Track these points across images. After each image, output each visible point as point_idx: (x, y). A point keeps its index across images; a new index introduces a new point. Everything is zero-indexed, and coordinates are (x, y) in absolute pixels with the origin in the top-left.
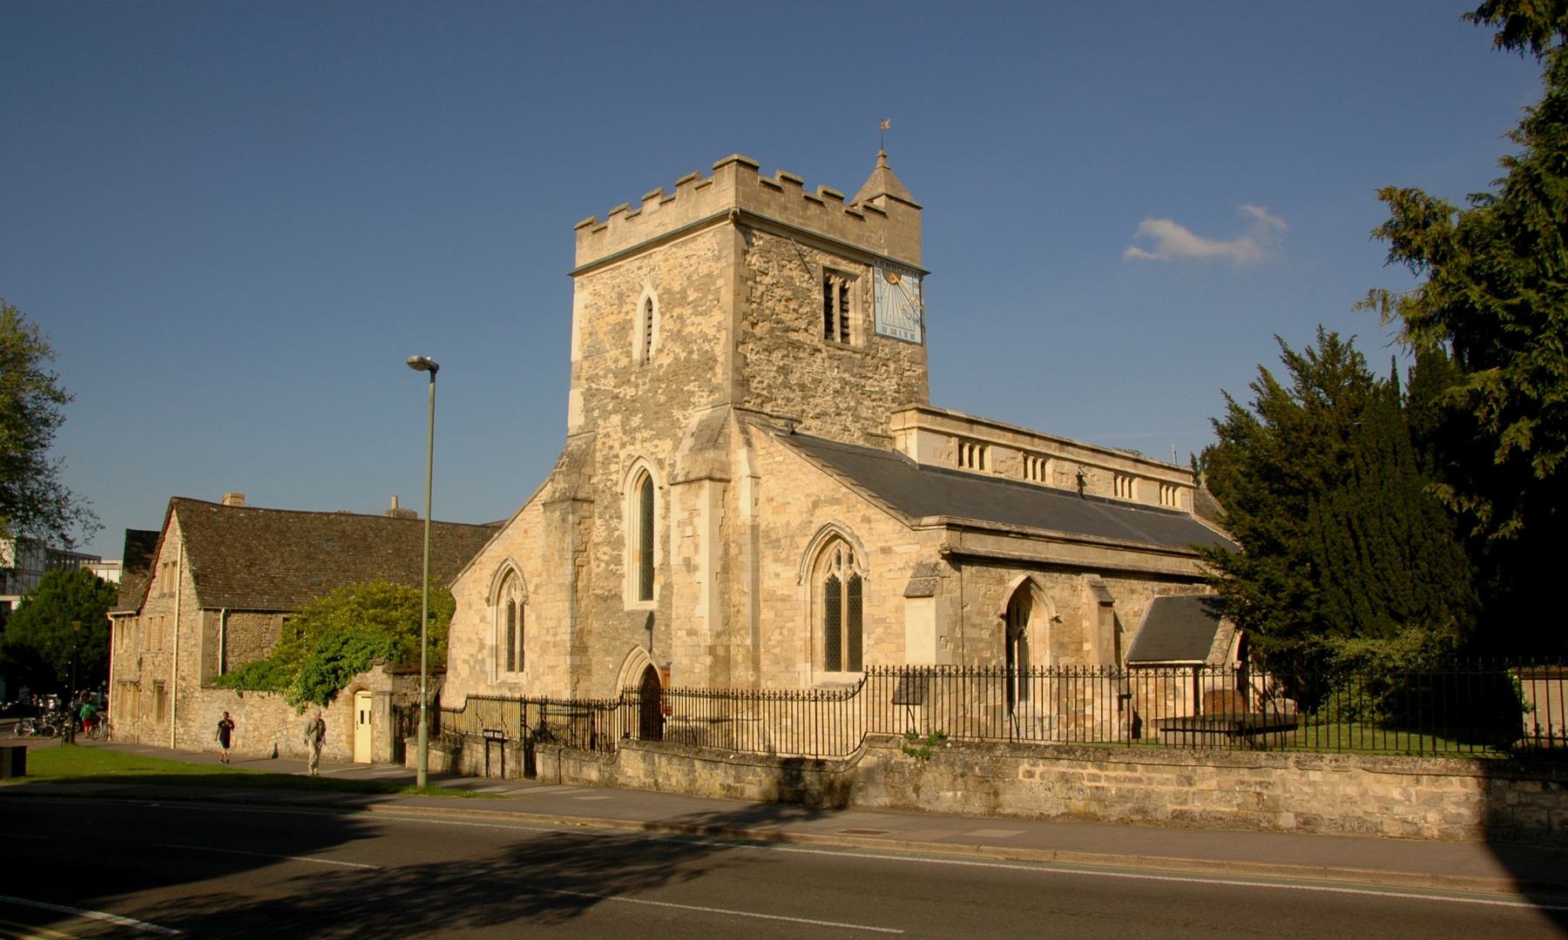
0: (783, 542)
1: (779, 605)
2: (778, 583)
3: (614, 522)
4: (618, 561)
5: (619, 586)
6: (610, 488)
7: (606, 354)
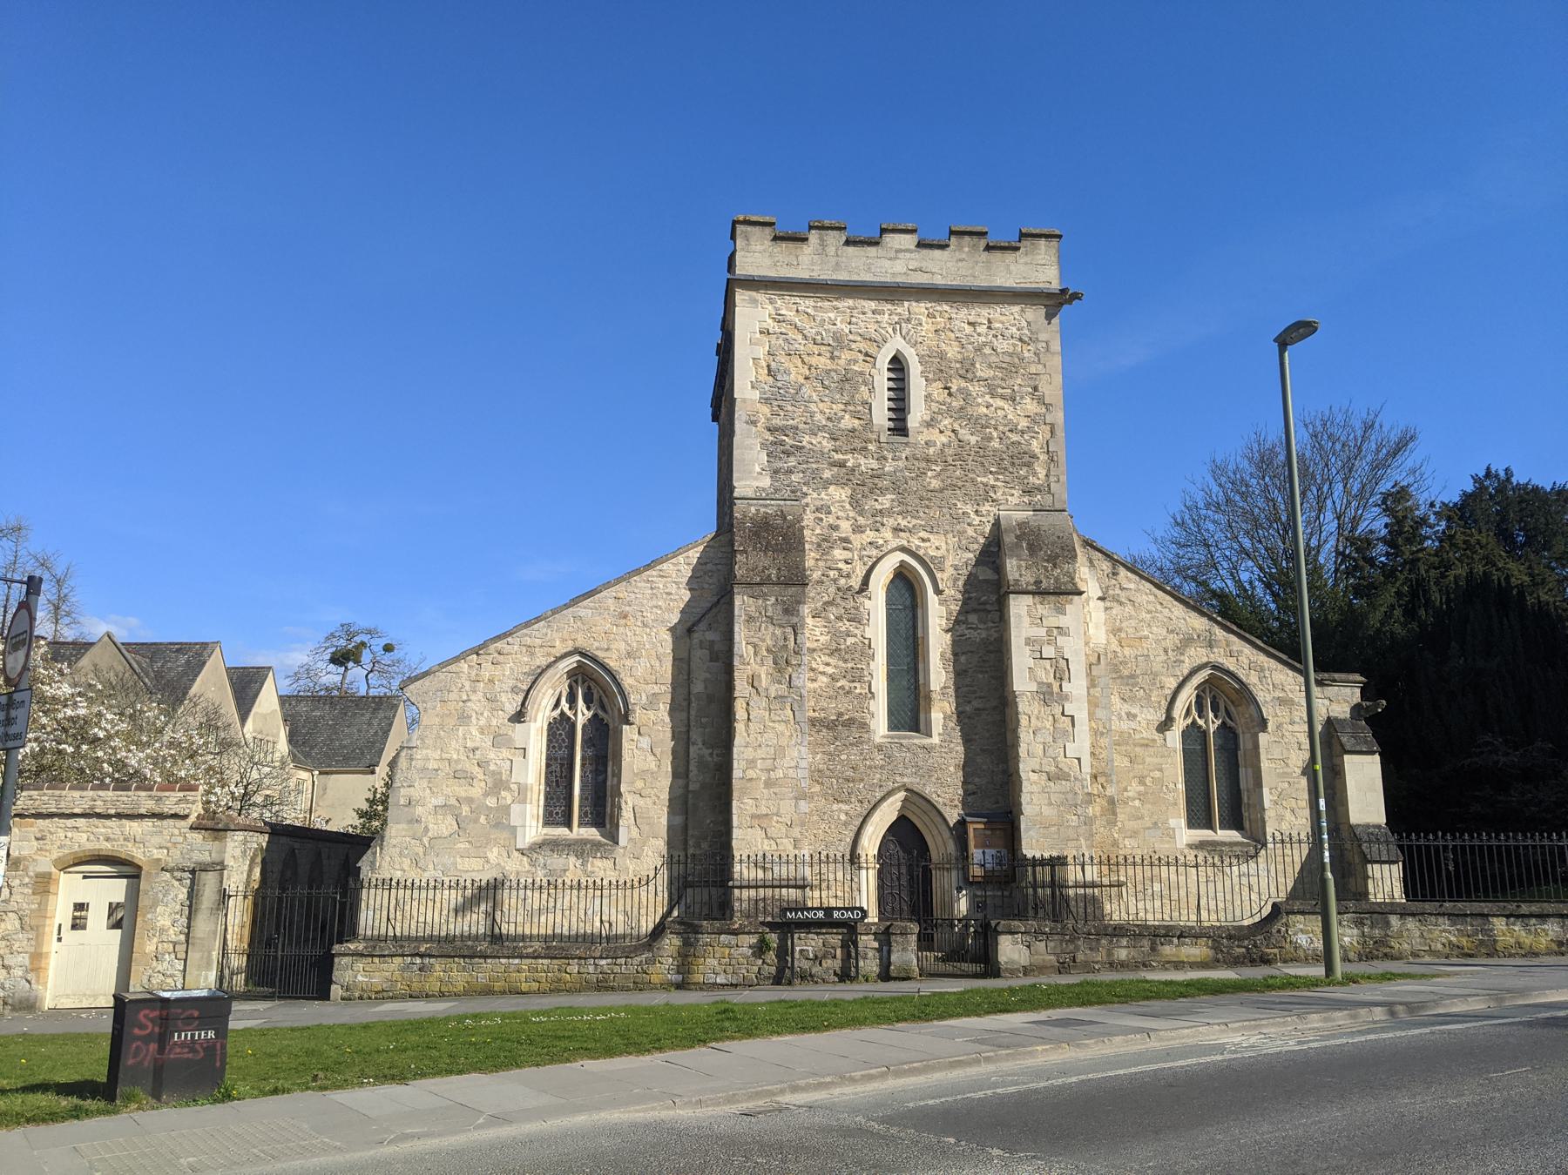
2: (1133, 725)
3: (844, 626)
4: (857, 676)
7: (811, 405)
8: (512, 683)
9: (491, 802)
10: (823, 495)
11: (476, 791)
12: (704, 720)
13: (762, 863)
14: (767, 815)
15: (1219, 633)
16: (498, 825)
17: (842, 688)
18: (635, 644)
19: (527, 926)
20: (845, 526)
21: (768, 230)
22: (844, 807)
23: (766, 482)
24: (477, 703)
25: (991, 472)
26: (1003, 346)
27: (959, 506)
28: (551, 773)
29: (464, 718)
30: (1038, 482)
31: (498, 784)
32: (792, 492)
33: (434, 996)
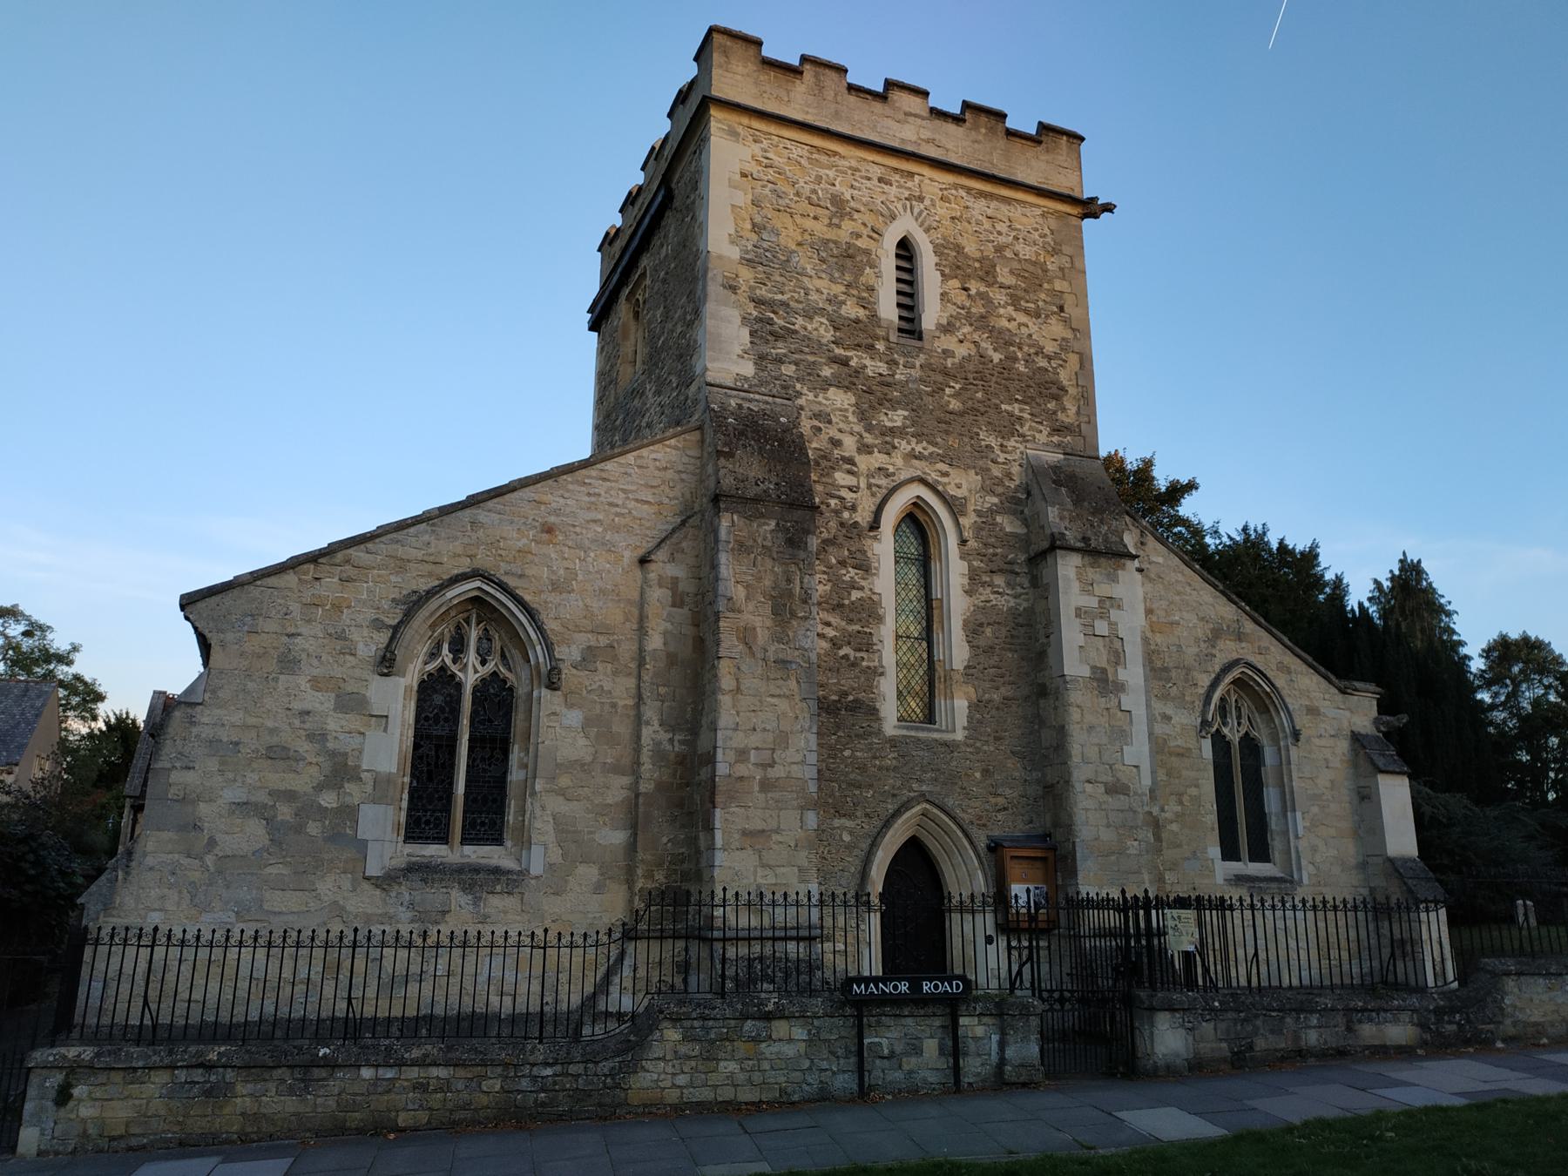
0: (1173, 674)
1: (1175, 761)
3: (851, 574)
4: (866, 644)
5: (870, 688)
6: (837, 512)
7: (805, 280)
8: (370, 614)
9: (328, 800)
10: (820, 399)
11: (303, 781)
12: (662, 690)
13: (757, 901)
14: (763, 831)
15: (1249, 626)
16: (335, 837)
17: (846, 657)
18: (562, 572)
19: (384, 1003)
20: (850, 443)
21: (752, 50)
22: (848, 823)
23: (748, 369)
24: (310, 639)
25: (1017, 399)
26: (1026, 252)
27: (981, 437)
28: (421, 758)
29: (288, 663)
30: (1067, 420)
31: (341, 771)
32: (784, 387)
33: (228, 1142)
